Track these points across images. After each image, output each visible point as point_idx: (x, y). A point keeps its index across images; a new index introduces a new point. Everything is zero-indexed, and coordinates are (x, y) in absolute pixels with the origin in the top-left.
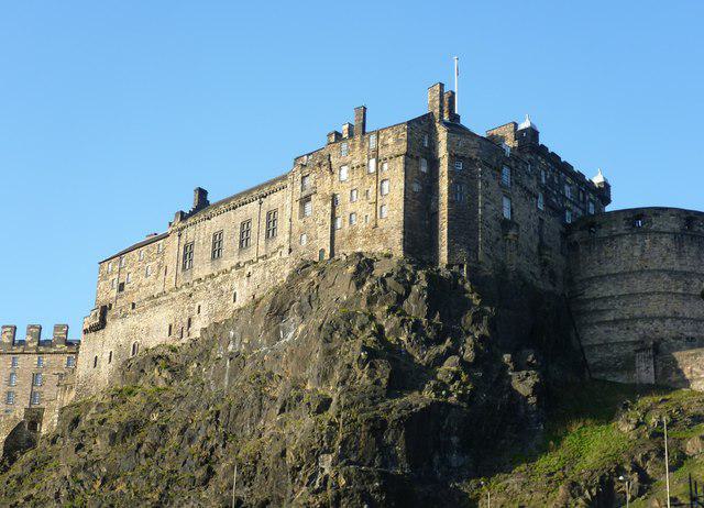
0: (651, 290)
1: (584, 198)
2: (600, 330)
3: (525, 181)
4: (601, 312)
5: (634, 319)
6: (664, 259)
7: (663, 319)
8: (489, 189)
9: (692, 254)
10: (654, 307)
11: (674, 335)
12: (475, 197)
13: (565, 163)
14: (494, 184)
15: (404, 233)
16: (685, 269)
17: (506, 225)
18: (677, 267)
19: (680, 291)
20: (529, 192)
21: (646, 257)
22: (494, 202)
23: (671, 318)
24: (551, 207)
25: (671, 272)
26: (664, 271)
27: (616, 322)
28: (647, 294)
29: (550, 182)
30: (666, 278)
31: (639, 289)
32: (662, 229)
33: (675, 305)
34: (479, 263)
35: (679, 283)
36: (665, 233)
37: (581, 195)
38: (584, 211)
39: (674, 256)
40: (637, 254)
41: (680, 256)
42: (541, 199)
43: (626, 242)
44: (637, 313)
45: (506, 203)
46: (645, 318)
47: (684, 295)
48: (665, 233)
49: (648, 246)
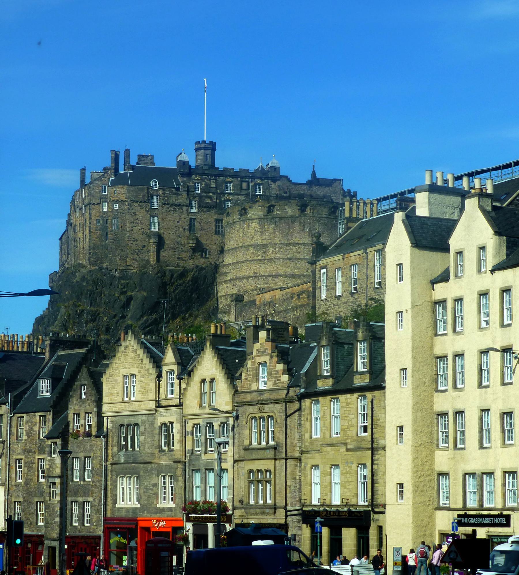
0: (244, 259)
1: (248, 186)
2: (225, 285)
3: (173, 199)
4: (226, 274)
5: (237, 279)
6: (253, 238)
7: (247, 278)
8: (137, 217)
9: (271, 231)
10: (246, 271)
11: (253, 288)
12: (124, 225)
13: (226, 169)
14: (141, 213)
15: (90, 253)
16: (265, 242)
17: (150, 235)
18: (259, 242)
19: (260, 258)
20: (179, 206)
21: (245, 236)
22: (141, 223)
23: (252, 277)
24: (205, 207)
25: (255, 246)
26: (252, 245)
27: (230, 281)
28: (242, 262)
29: (207, 189)
30: (252, 250)
31: (240, 259)
32: (253, 217)
33: (256, 268)
34: (128, 266)
35: (259, 253)
36: (254, 219)
37: (244, 185)
38: (247, 195)
39: (259, 234)
40: (241, 235)
41: (262, 233)
42: (195, 204)
43: (238, 226)
44: (238, 275)
45: (155, 221)
46: (241, 279)
47: (260, 260)
48: (254, 219)
49: (245, 229)
